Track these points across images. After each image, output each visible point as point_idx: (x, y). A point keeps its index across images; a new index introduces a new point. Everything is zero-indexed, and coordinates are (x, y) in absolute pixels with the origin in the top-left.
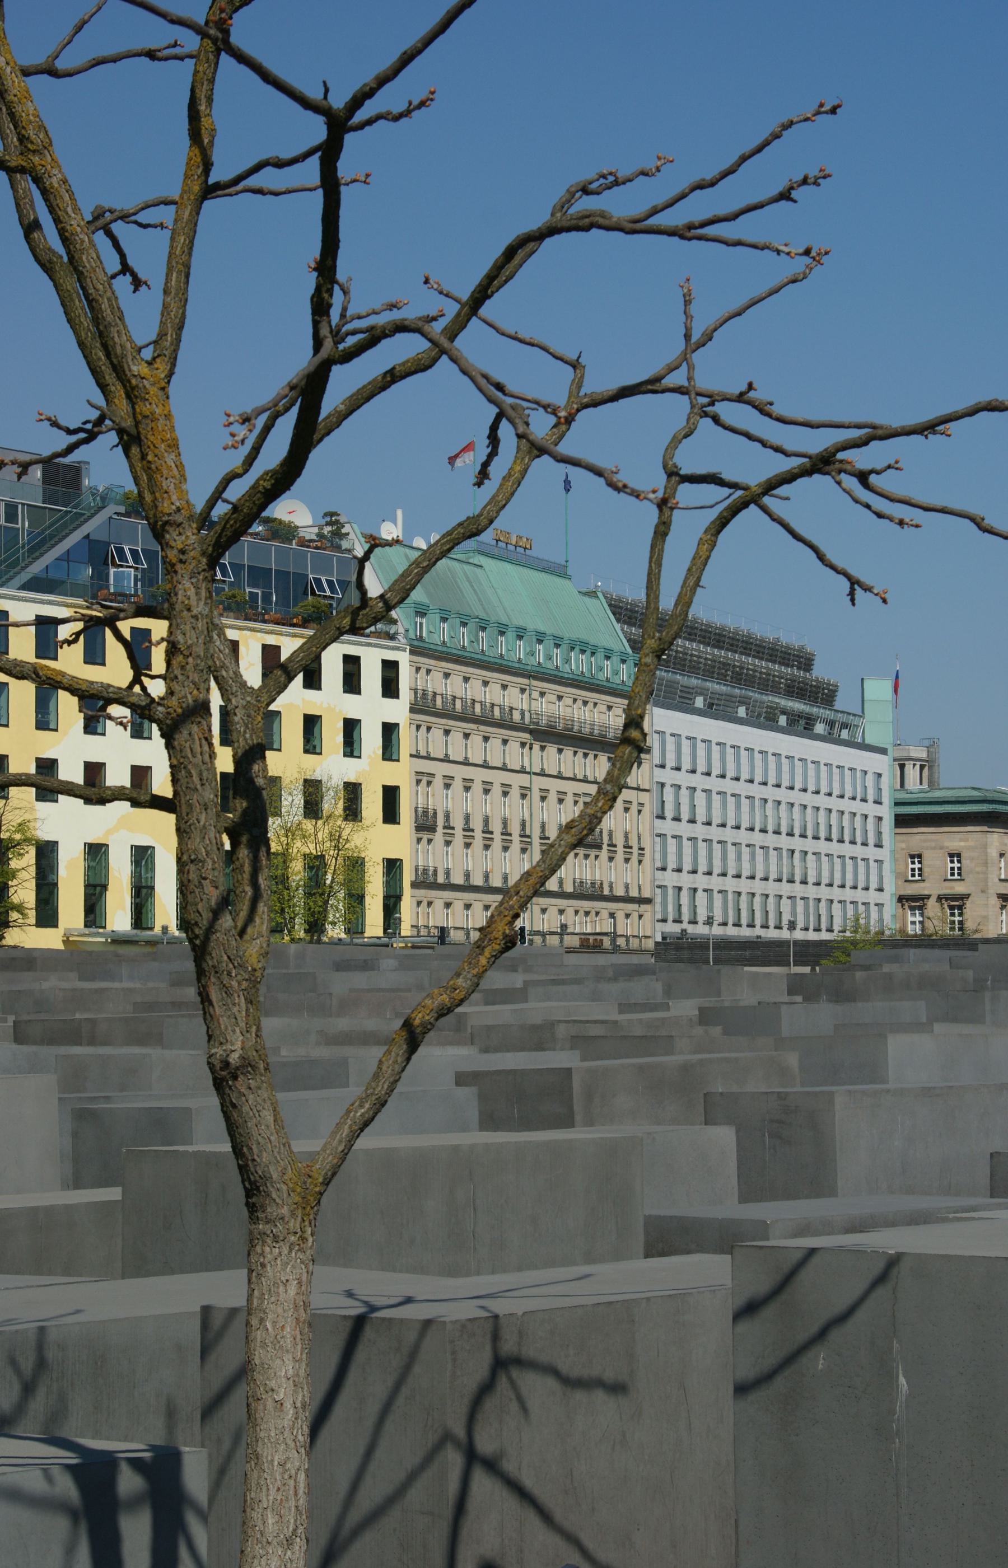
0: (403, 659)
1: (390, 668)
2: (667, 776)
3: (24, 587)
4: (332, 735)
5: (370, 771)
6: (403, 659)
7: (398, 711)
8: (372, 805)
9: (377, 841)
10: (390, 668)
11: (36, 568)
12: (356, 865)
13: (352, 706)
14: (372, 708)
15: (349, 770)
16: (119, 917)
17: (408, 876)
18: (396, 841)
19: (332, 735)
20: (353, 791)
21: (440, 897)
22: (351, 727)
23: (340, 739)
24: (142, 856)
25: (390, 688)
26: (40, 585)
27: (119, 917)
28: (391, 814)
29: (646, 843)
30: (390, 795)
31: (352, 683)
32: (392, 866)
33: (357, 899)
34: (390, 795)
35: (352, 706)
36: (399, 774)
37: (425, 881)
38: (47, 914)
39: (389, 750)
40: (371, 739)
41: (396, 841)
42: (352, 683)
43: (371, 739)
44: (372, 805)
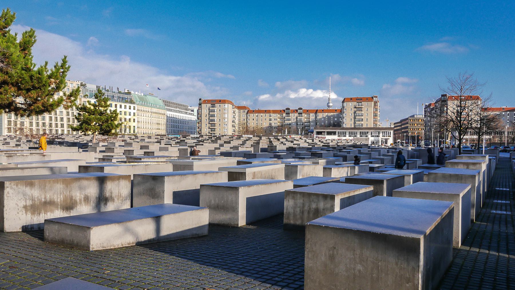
0: (136, 106)
1: (134, 107)
4: (128, 114)
5: (132, 117)
7: (135, 111)
8: (132, 120)
9: (132, 124)
10: (134, 107)
12: (130, 126)
14: (132, 111)
15: (130, 117)
17: (136, 127)
18: (135, 124)
19: (128, 114)
20: (130, 120)
21: (140, 130)
28: (134, 121)
30: (134, 119)
31: (130, 109)
33: (130, 129)
34: (134, 119)
35: (130, 111)
36: (134, 117)
37: (138, 127)
40: (132, 114)
41: (135, 124)
42: (130, 109)
43: (132, 114)
44: (132, 120)
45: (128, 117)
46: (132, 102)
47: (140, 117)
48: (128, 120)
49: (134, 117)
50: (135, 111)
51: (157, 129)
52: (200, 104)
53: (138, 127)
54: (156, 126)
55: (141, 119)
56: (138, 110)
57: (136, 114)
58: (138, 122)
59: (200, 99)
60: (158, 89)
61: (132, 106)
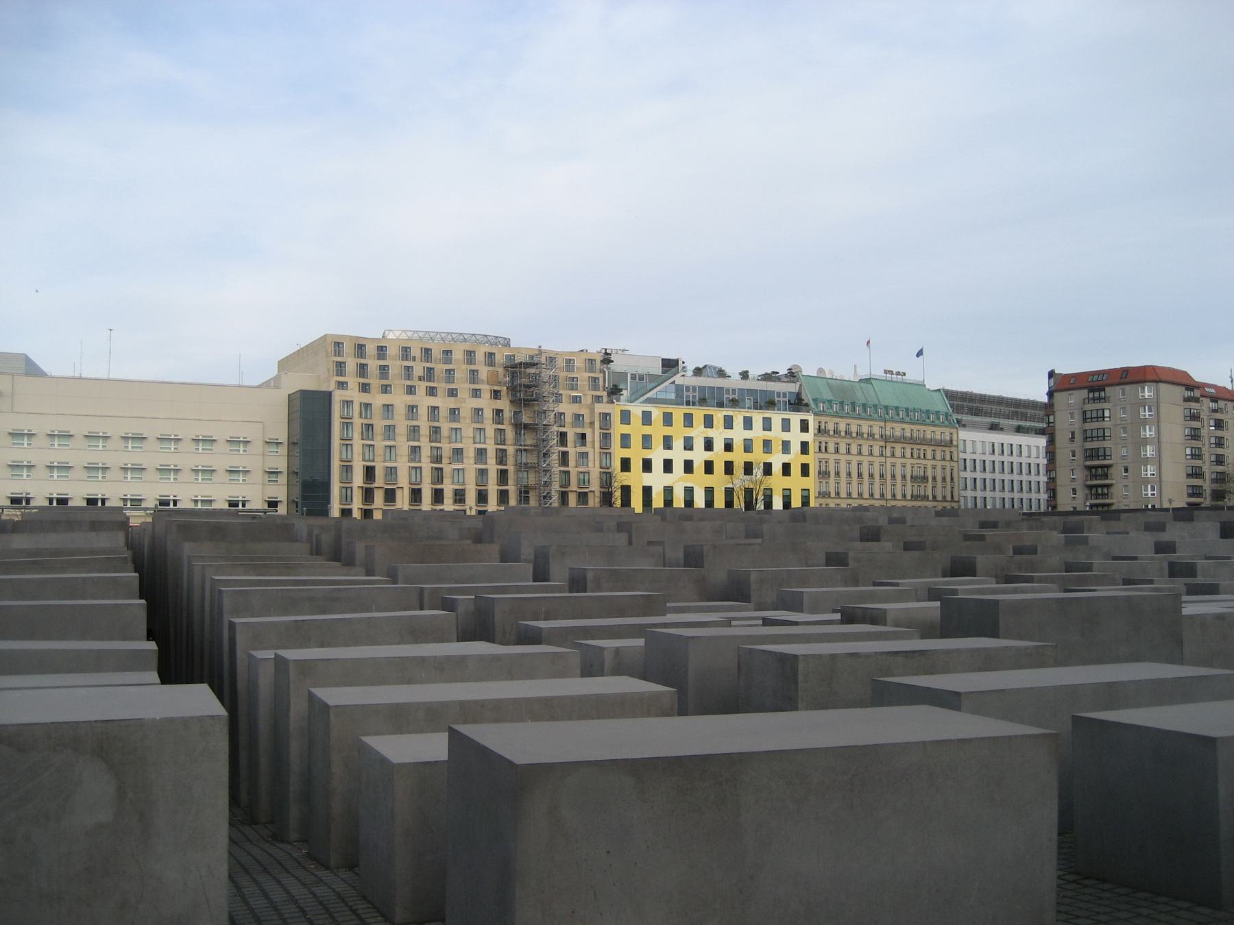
0: (810, 418)
2: (969, 457)
4: (777, 446)
5: (795, 458)
6: (810, 418)
7: (808, 437)
11: (648, 395)
13: (786, 436)
14: (796, 437)
18: (810, 483)
19: (777, 446)
25: (804, 427)
29: (956, 480)
34: (805, 470)
36: (809, 459)
43: (796, 448)
45: (777, 460)
46: (797, 403)
47: (832, 458)
49: (805, 459)
50: (808, 437)
52: (1050, 394)
53: (823, 495)
55: (838, 461)
56: (820, 431)
57: (812, 448)
58: (823, 474)
59: (1051, 374)
60: (920, 354)
61: (795, 419)
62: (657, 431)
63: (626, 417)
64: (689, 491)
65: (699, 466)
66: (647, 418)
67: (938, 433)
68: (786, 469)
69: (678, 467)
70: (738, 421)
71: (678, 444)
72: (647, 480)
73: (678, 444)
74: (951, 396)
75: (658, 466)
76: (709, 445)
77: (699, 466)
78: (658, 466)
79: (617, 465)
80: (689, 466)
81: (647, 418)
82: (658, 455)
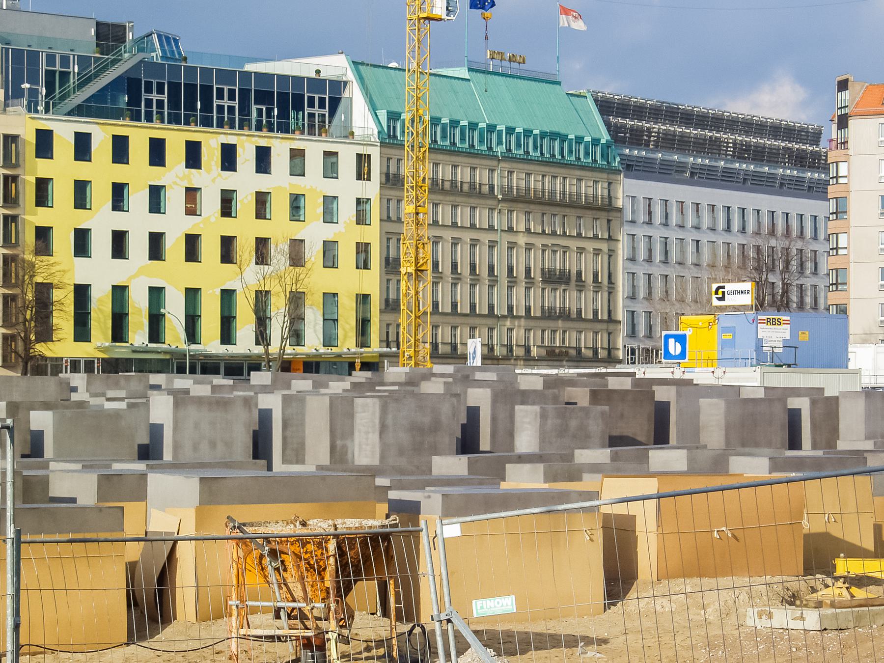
3: (70, 113)
4: (313, 208)
12: (330, 298)
15: (329, 232)
16: (138, 335)
22: (329, 202)
23: (320, 210)
24: (156, 294)
26: (80, 111)
27: (138, 335)
32: (364, 299)
33: (330, 321)
34: (363, 249)
38: (82, 332)
39: (361, 219)
43: (346, 210)
45: (314, 232)
48: (313, 253)
51: (549, 315)
54: (540, 298)
62: (101, 171)
63: (44, 143)
64: (156, 294)
65: (174, 246)
66: (83, 147)
67: (588, 188)
68: (329, 251)
69: (138, 246)
70: (246, 157)
71: (138, 199)
72: (81, 271)
73: (138, 199)
74: (606, 107)
75: (101, 244)
76: (156, 196)
77: (174, 246)
78: (101, 244)
79: (29, 238)
80: (119, 244)
81: (83, 147)
82: (101, 221)
